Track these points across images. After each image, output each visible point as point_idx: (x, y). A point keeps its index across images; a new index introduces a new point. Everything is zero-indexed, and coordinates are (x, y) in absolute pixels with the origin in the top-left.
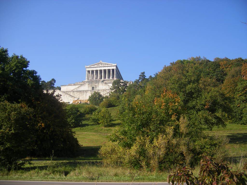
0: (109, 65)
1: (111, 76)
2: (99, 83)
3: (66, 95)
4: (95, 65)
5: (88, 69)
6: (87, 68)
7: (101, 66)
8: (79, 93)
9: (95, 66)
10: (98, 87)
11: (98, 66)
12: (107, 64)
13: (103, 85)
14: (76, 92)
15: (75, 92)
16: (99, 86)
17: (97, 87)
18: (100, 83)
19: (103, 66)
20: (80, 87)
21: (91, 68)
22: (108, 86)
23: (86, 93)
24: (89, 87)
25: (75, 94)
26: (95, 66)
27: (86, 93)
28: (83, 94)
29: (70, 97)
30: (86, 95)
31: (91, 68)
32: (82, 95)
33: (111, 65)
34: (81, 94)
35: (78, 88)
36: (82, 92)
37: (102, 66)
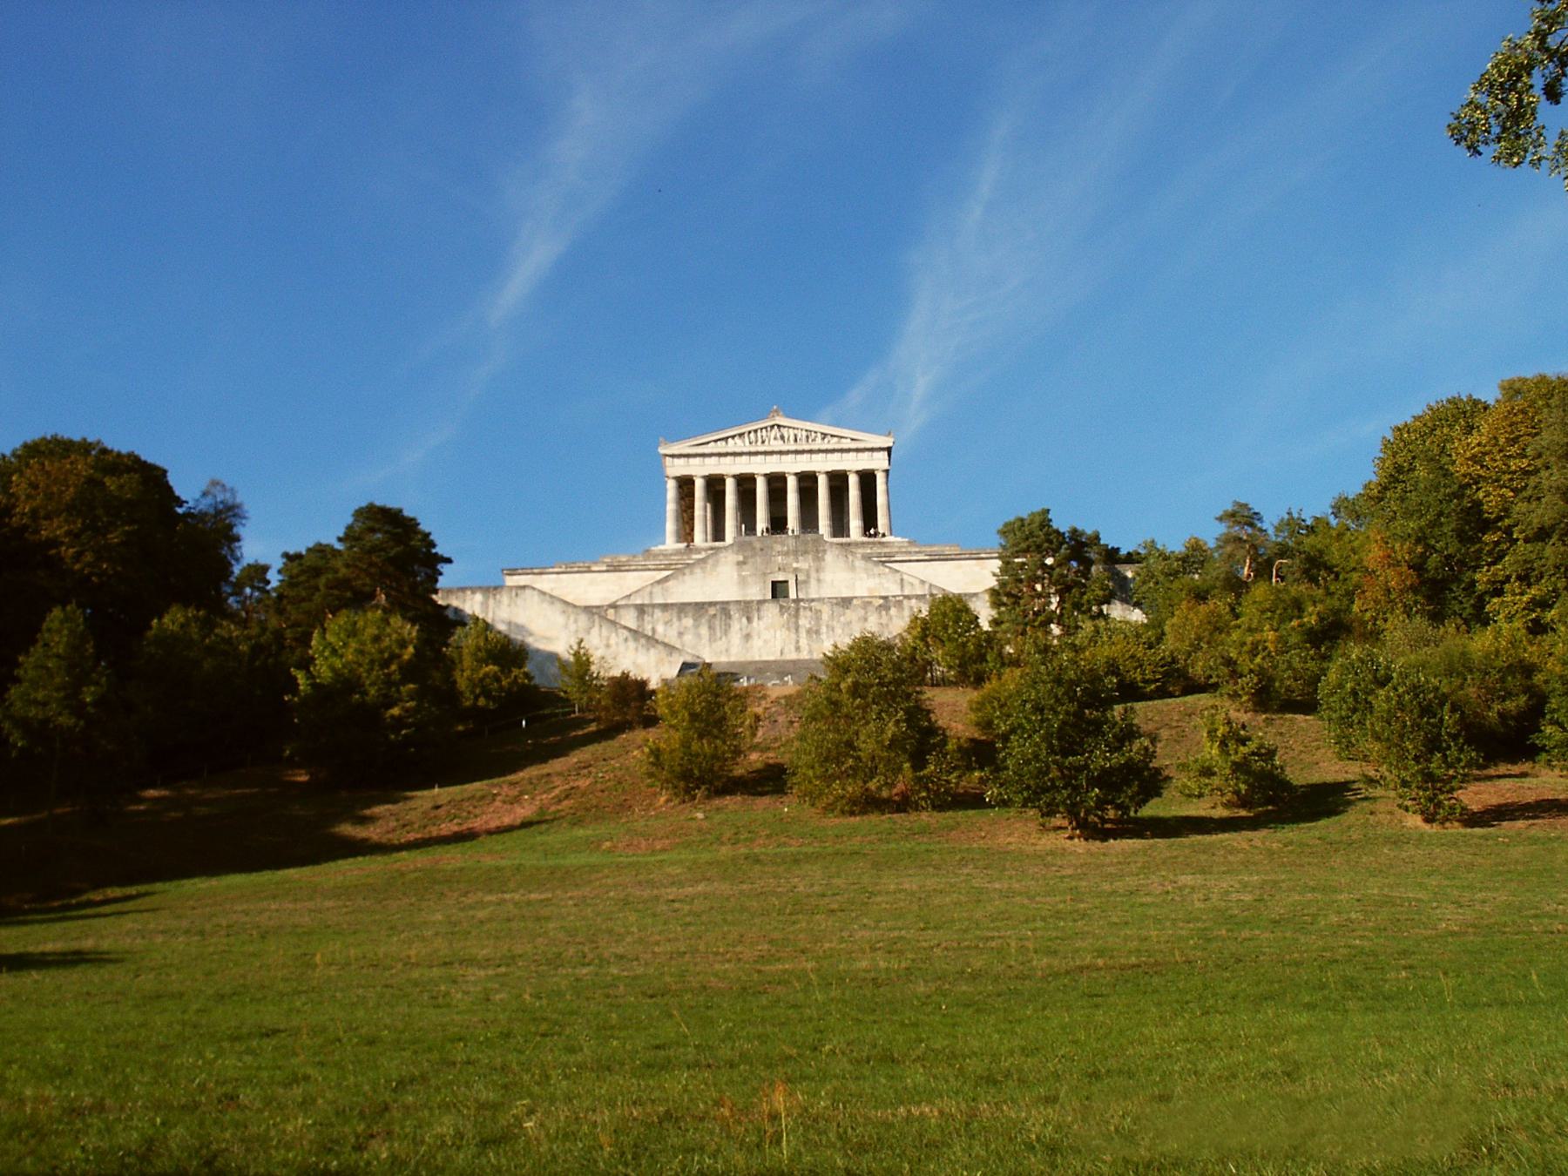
0: (833, 443)
1: (855, 522)
2: (825, 551)
3: (595, 631)
4: (733, 437)
5: (678, 468)
6: (673, 456)
7: (778, 445)
8: (688, 622)
9: (732, 446)
10: (813, 582)
11: (753, 449)
12: (824, 435)
13: (853, 568)
14: (667, 616)
15: (658, 613)
16: (827, 576)
17: (806, 582)
18: (829, 557)
19: (793, 447)
20: (670, 583)
21: (703, 455)
22: (898, 576)
23: (749, 620)
24: (743, 581)
25: (660, 629)
26: (732, 446)
27: (749, 620)
28: (726, 632)
29: (632, 644)
30: (748, 637)
31: (703, 455)
32: (712, 639)
33: (854, 445)
34: (704, 631)
35: (657, 589)
36: (712, 611)
37: (785, 448)
